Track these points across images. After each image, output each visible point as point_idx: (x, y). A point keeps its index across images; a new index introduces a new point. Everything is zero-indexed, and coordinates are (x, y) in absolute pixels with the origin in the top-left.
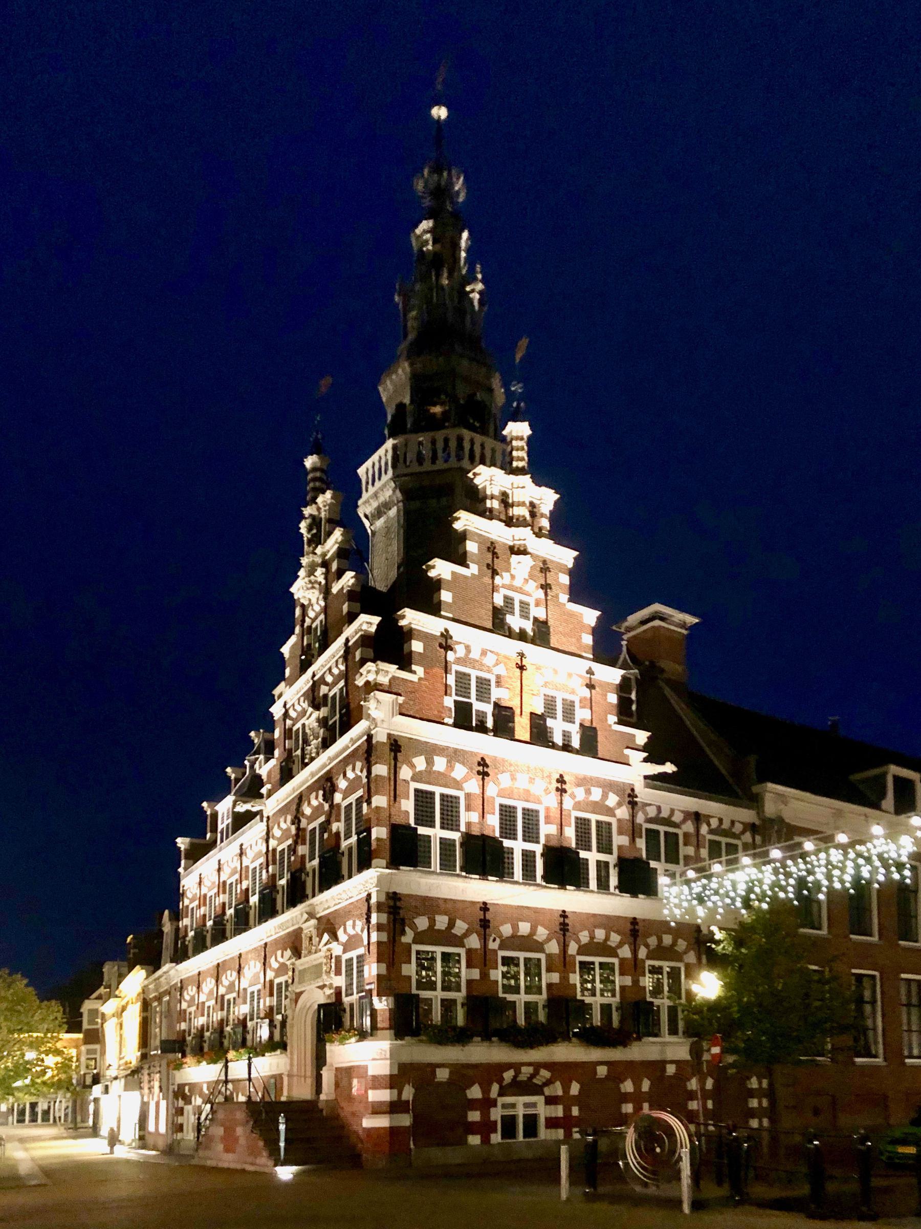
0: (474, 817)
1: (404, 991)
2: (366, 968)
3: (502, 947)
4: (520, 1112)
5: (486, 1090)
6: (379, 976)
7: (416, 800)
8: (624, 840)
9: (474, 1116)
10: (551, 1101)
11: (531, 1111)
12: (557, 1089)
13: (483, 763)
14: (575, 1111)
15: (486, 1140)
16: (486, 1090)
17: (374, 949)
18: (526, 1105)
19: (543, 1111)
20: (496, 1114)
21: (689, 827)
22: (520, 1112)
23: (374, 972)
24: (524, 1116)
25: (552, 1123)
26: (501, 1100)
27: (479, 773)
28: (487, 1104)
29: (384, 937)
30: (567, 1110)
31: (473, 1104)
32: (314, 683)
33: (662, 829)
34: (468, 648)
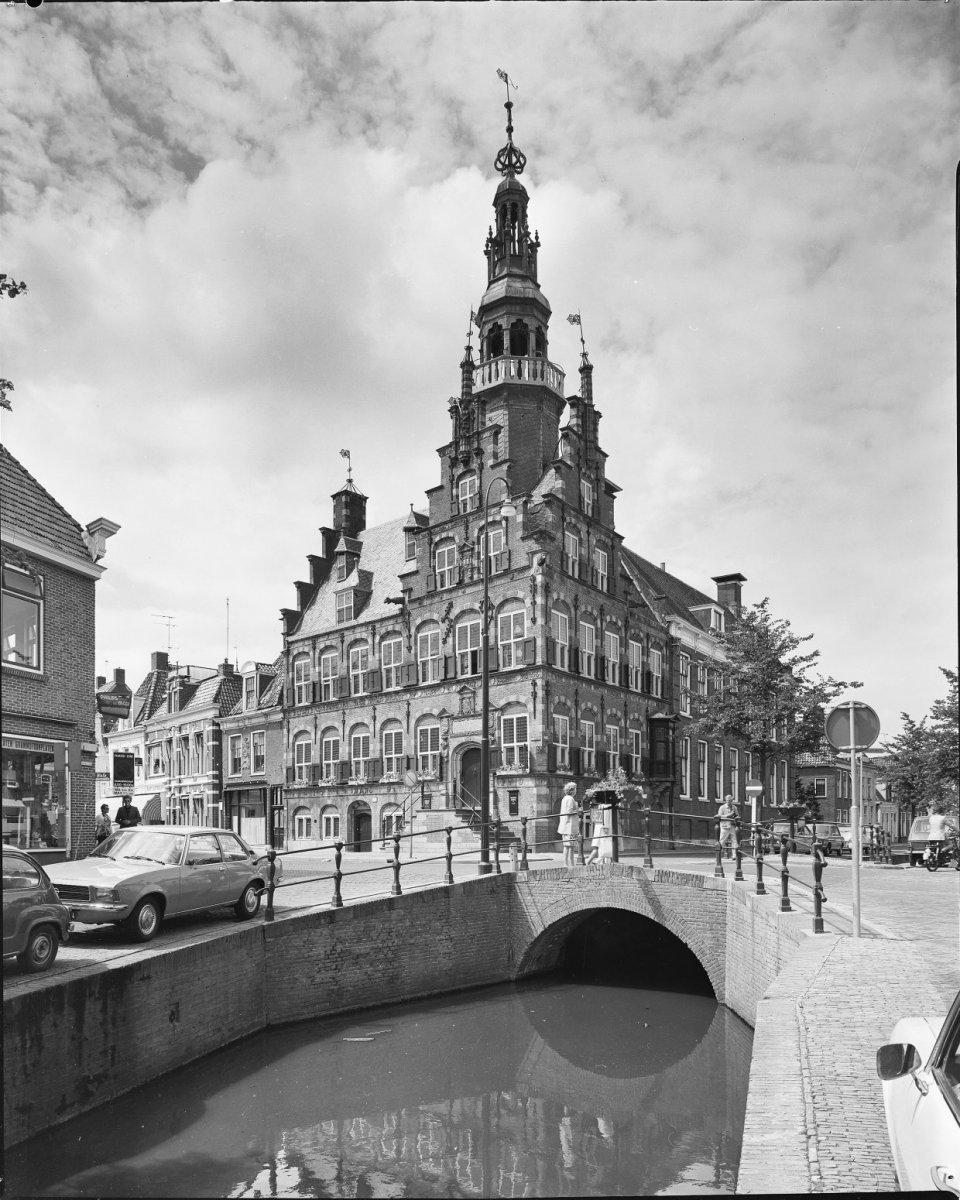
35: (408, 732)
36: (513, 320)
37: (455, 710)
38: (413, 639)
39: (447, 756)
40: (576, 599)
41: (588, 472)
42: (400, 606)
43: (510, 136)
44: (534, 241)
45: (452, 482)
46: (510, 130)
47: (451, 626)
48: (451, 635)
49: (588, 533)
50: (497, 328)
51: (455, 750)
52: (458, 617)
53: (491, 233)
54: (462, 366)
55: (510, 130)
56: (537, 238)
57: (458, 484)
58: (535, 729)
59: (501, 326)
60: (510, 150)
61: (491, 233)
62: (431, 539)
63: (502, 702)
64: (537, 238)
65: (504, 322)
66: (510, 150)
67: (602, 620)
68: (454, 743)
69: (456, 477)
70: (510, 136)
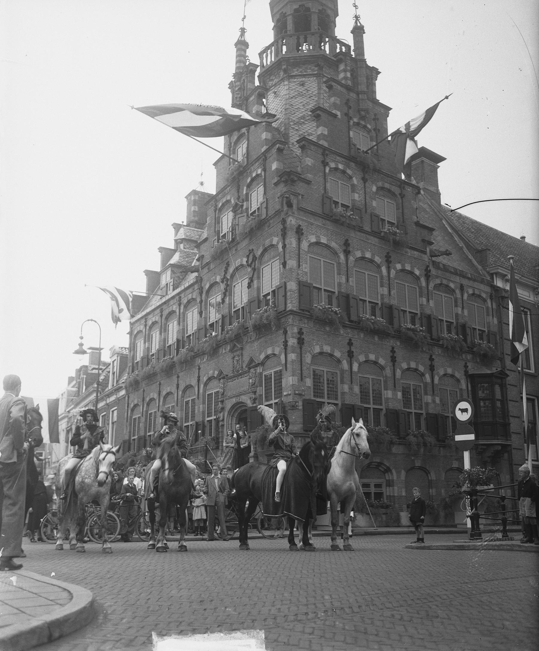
11: (378, 490)
18: (378, 486)
24: (375, 493)
35: (198, 398)
37: (228, 371)
38: (203, 304)
39: (223, 420)
40: (346, 244)
41: (363, 123)
42: (196, 274)
45: (230, 150)
47: (227, 285)
48: (228, 293)
49: (365, 180)
51: (229, 412)
52: (232, 276)
54: (236, 45)
57: (234, 149)
62: (216, 206)
63: (262, 356)
67: (389, 269)
68: (229, 405)
69: (233, 144)
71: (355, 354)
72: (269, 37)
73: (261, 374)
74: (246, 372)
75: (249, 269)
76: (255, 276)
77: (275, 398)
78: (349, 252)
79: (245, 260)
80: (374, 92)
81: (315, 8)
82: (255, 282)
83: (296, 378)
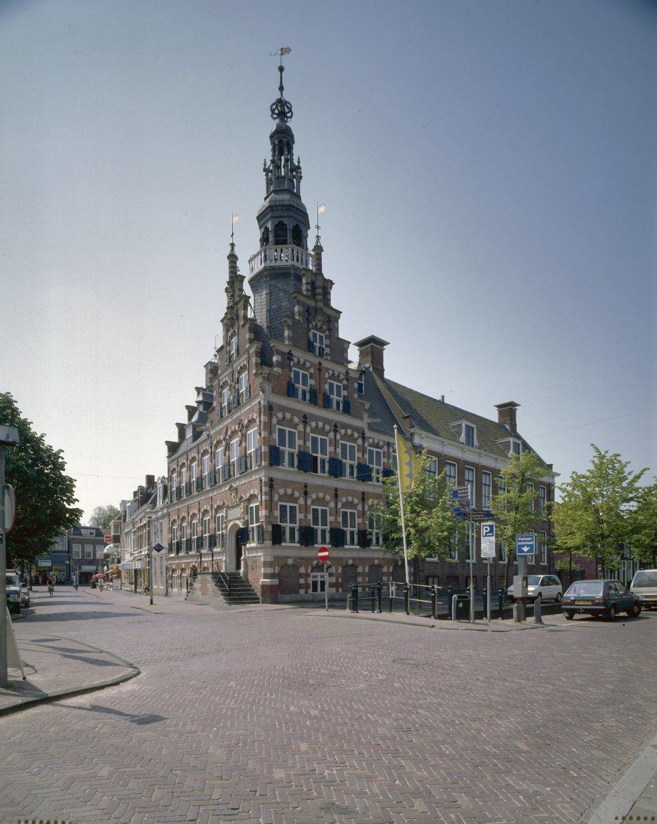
0: (301, 442)
1: (275, 523)
2: (260, 512)
3: (313, 503)
4: (319, 579)
5: (307, 570)
6: (266, 516)
7: (279, 434)
8: (360, 455)
9: (302, 581)
10: (331, 575)
11: (323, 579)
12: (333, 570)
13: (305, 417)
14: (340, 580)
15: (307, 592)
16: (307, 570)
17: (263, 503)
19: (328, 580)
20: (310, 580)
21: (385, 448)
22: (319, 579)
23: (264, 514)
24: (321, 582)
25: (331, 585)
26: (312, 574)
27: (303, 422)
28: (307, 575)
29: (268, 498)
30: (337, 579)
31: (301, 575)
32: (233, 371)
33: (375, 450)
34: (299, 359)
36: (277, 221)
43: (282, 94)
44: (297, 164)
46: (281, 88)
50: (267, 229)
53: (265, 165)
54: (228, 257)
55: (281, 88)
56: (299, 162)
58: (263, 513)
59: (268, 228)
60: (281, 103)
61: (265, 165)
64: (299, 162)
65: (269, 225)
66: (281, 103)
70: (282, 94)
71: (309, 493)
72: (256, 246)
73: (247, 506)
74: (237, 505)
75: (240, 434)
76: (243, 439)
77: (256, 523)
78: (307, 422)
79: (237, 426)
80: (329, 300)
81: (290, 224)
82: (244, 443)
83: (267, 512)
